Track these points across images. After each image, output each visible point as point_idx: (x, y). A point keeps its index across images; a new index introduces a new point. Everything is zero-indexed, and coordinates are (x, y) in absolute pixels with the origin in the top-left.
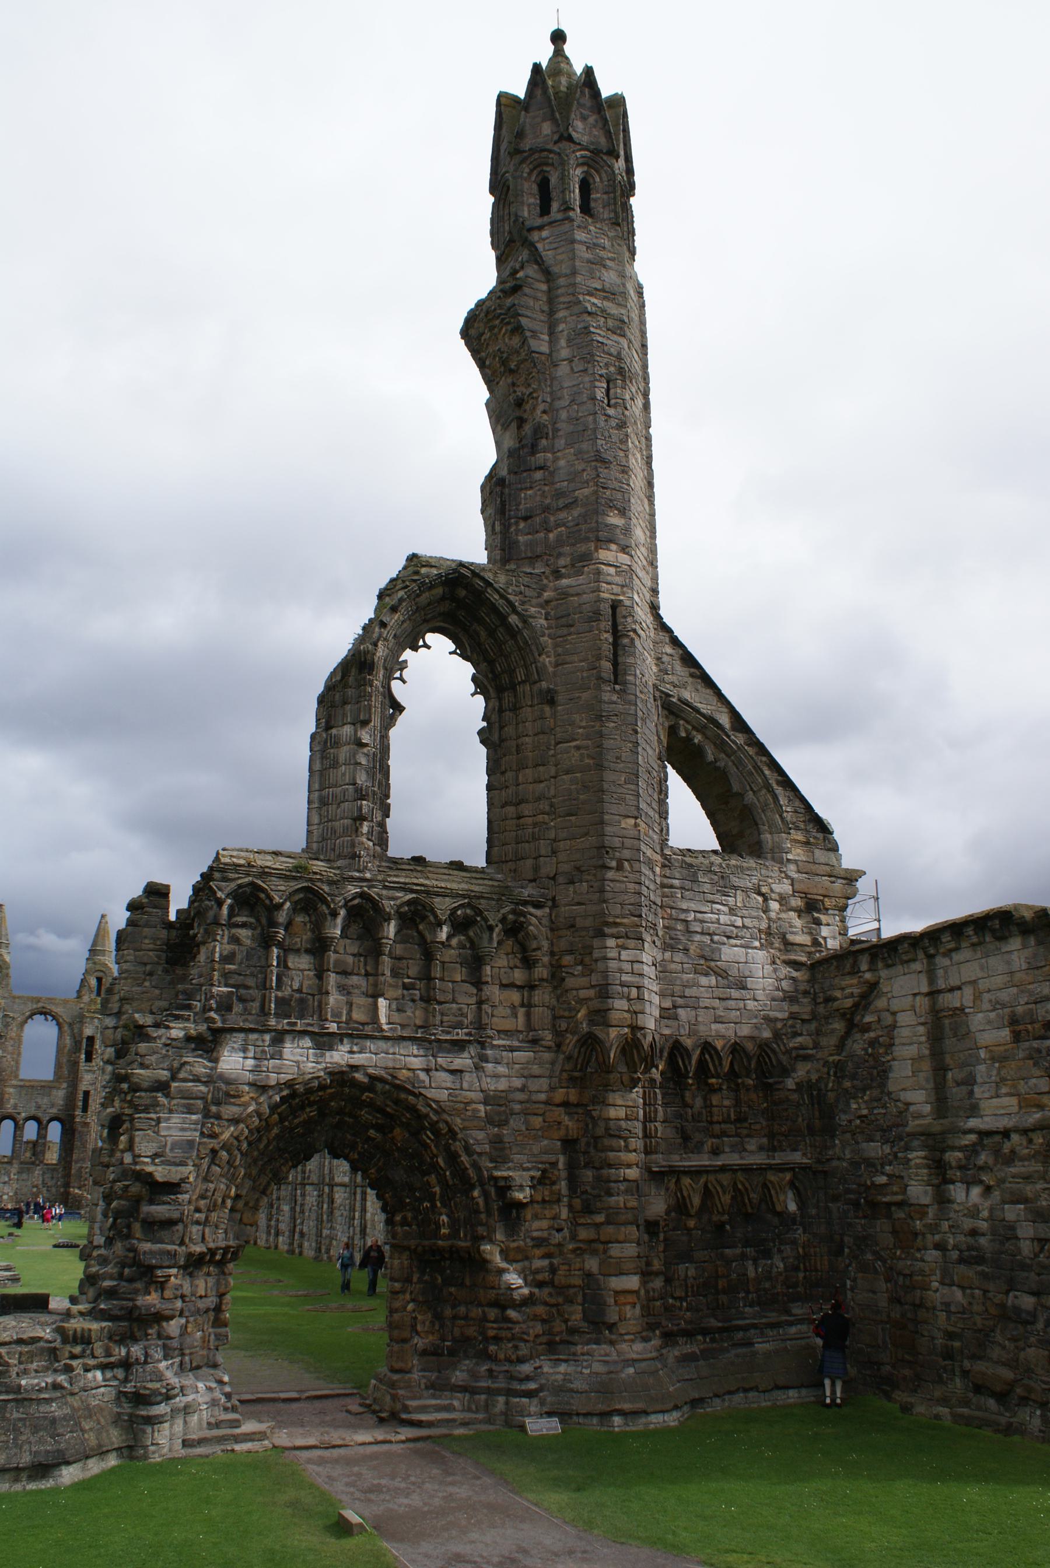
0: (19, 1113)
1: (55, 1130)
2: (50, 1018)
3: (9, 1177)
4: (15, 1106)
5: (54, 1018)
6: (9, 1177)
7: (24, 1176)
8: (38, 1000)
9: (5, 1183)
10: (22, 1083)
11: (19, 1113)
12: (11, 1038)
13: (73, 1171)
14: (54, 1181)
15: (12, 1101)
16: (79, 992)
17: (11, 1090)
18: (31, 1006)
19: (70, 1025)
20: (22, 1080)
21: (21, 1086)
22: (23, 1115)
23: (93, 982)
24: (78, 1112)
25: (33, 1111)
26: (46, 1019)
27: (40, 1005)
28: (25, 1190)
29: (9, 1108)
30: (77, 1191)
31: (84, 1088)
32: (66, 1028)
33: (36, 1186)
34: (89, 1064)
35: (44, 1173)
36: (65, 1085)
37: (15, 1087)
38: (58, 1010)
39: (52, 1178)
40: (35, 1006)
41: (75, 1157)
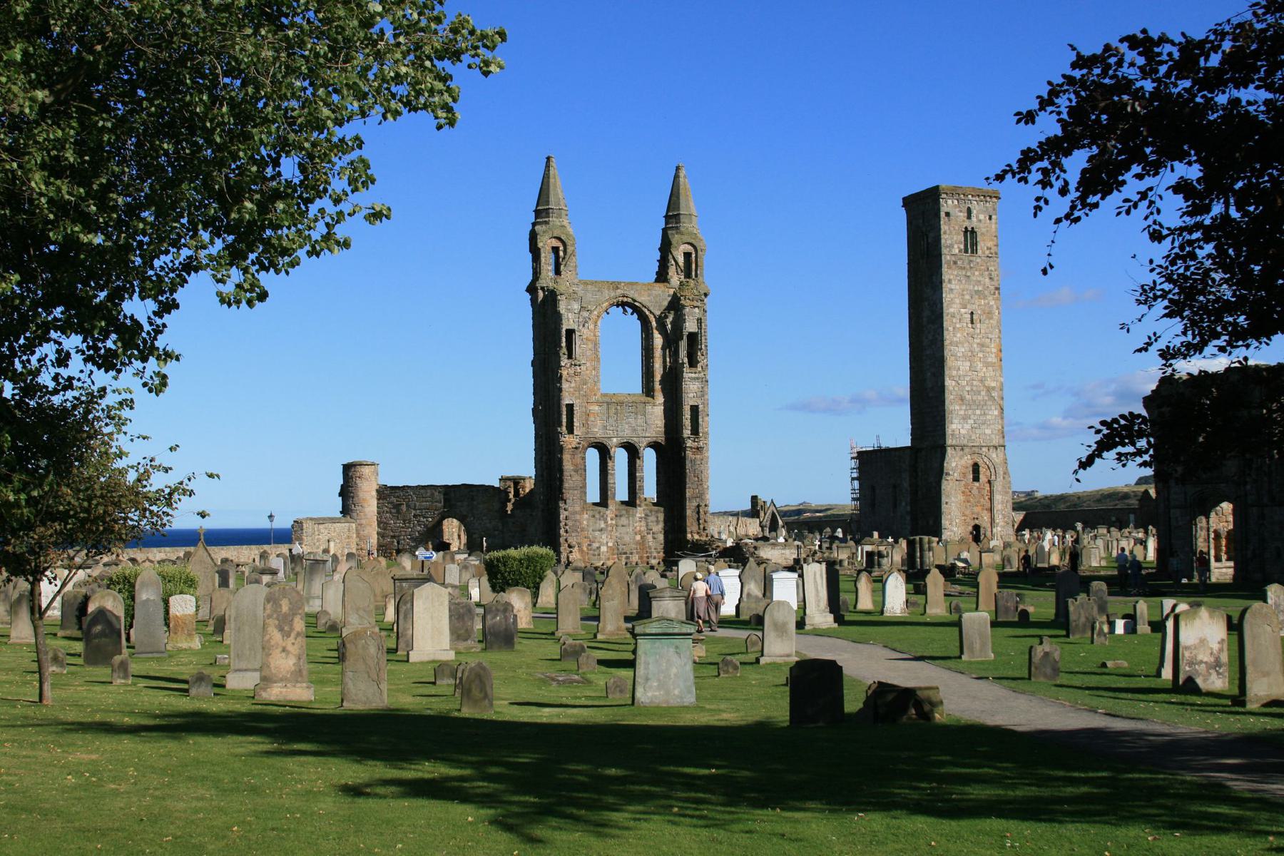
1: (649, 460)
2: (630, 310)
3: (606, 522)
5: (637, 310)
6: (606, 522)
7: (624, 521)
8: (616, 286)
10: (607, 399)
12: (587, 339)
13: (689, 512)
16: (662, 277)
17: (597, 408)
18: (609, 294)
20: (606, 395)
21: (608, 404)
23: (681, 260)
24: (687, 432)
25: (627, 434)
26: (625, 311)
27: (619, 292)
29: (598, 432)
30: (696, 537)
34: (693, 370)
35: (646, 515)
37: (599, 403)
38: (643, 298)
39: (657, 522)
40: (613, 294)
41: (688, 495)
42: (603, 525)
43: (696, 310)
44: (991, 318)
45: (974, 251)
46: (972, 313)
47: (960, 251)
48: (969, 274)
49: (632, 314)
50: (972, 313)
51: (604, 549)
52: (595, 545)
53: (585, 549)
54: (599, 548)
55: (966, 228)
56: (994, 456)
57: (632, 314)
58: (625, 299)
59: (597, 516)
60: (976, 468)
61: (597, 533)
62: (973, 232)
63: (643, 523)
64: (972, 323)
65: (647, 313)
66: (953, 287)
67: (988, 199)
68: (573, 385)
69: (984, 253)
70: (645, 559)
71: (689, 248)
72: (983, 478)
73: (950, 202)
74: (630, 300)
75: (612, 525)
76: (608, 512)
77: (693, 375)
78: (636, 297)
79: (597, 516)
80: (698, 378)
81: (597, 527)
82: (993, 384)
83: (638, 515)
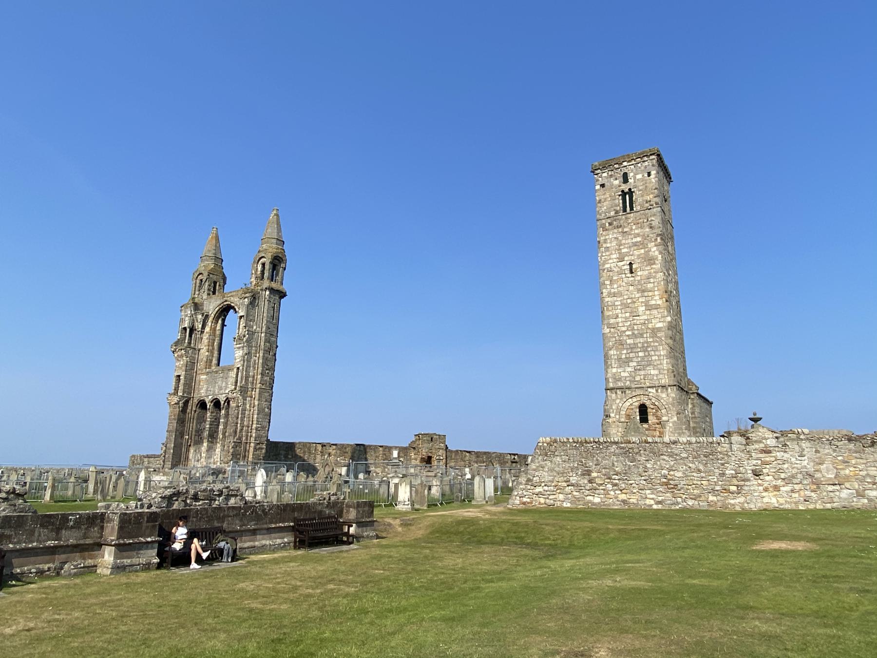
44: (654, 264)
45: (632, 208)
46: (631, 264)
47: (617, 212)
48: (625, 230)
50: (631, 264)
55: (623, 191)
56: (664, 395)
60: (643, 410)
62: (631, 192)
64: (631, 272)
66: (608, 245)
67: (646, 158)
69: (642, 206)
72: (651, 419)
73: (605, 175)
82: (660, 325)
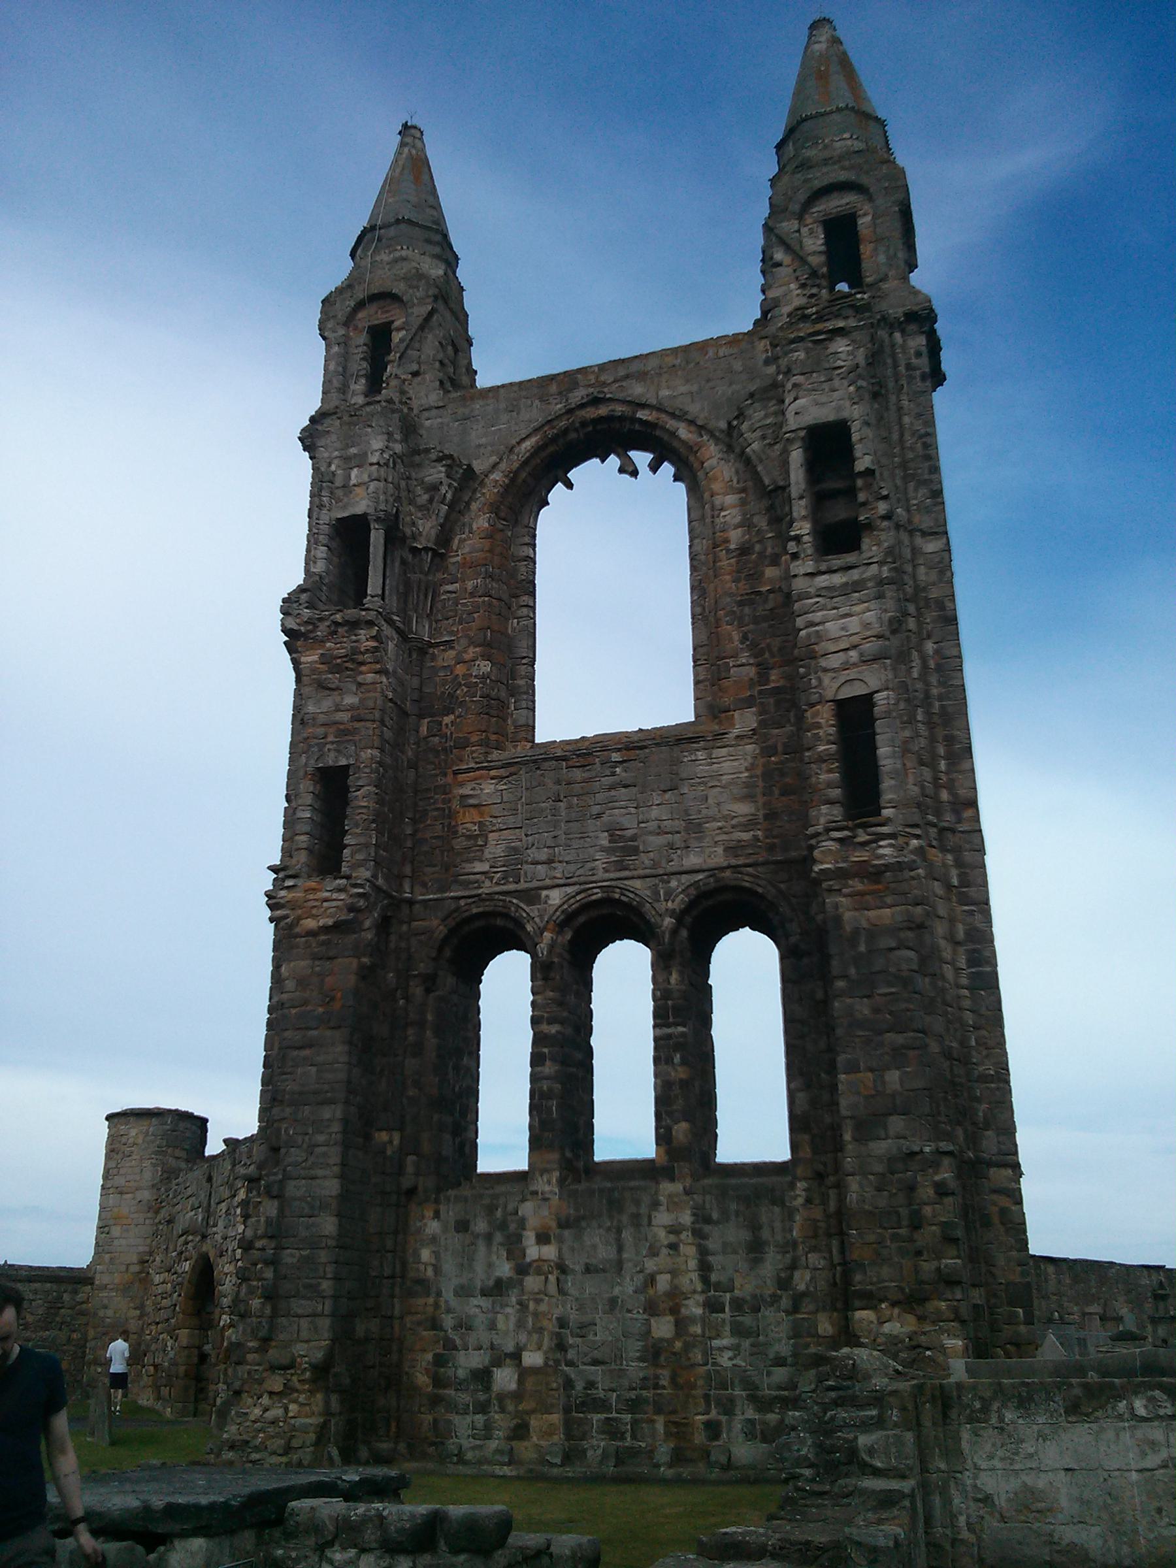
0: (531, 896)
2: (642, 459)
4: (515, 859)
6: (514, 1246)
8: (568, 380)
9: (498, 1289)
11: (531, 896)
14: (772, 1263)
15: (496, 847)
19: (730, 440)
22: (555, 897)
28: (604, 1331)
31: (832, 687)
32: (712, 454)
33: (674, 1302)
35: (702, 1217)
36: (745, 721)
39: (756, 1249)
42: (505, 1269)
43: (841, 346)
49: (654, 467)
51: (505, 1379)
52: (470, 1360)
53: (422, 1379)
54: (483, 1376)
57: (654, 467)
58: (603, 411)
59: (481, 1226)
61: (477, 1305)
63: (689, 1251)
65: (684, 432)
68: (350, 700)
70: (699, 1438)
71: (836, 204)
74: (619, 409)
75: (538, 1267)
76: (527, 1209)
77: (838, 579)
78: (637, 390)
79: (481, 1226)
80: (857, 587)
81: (480, 1276)
83: (663, 1218)
